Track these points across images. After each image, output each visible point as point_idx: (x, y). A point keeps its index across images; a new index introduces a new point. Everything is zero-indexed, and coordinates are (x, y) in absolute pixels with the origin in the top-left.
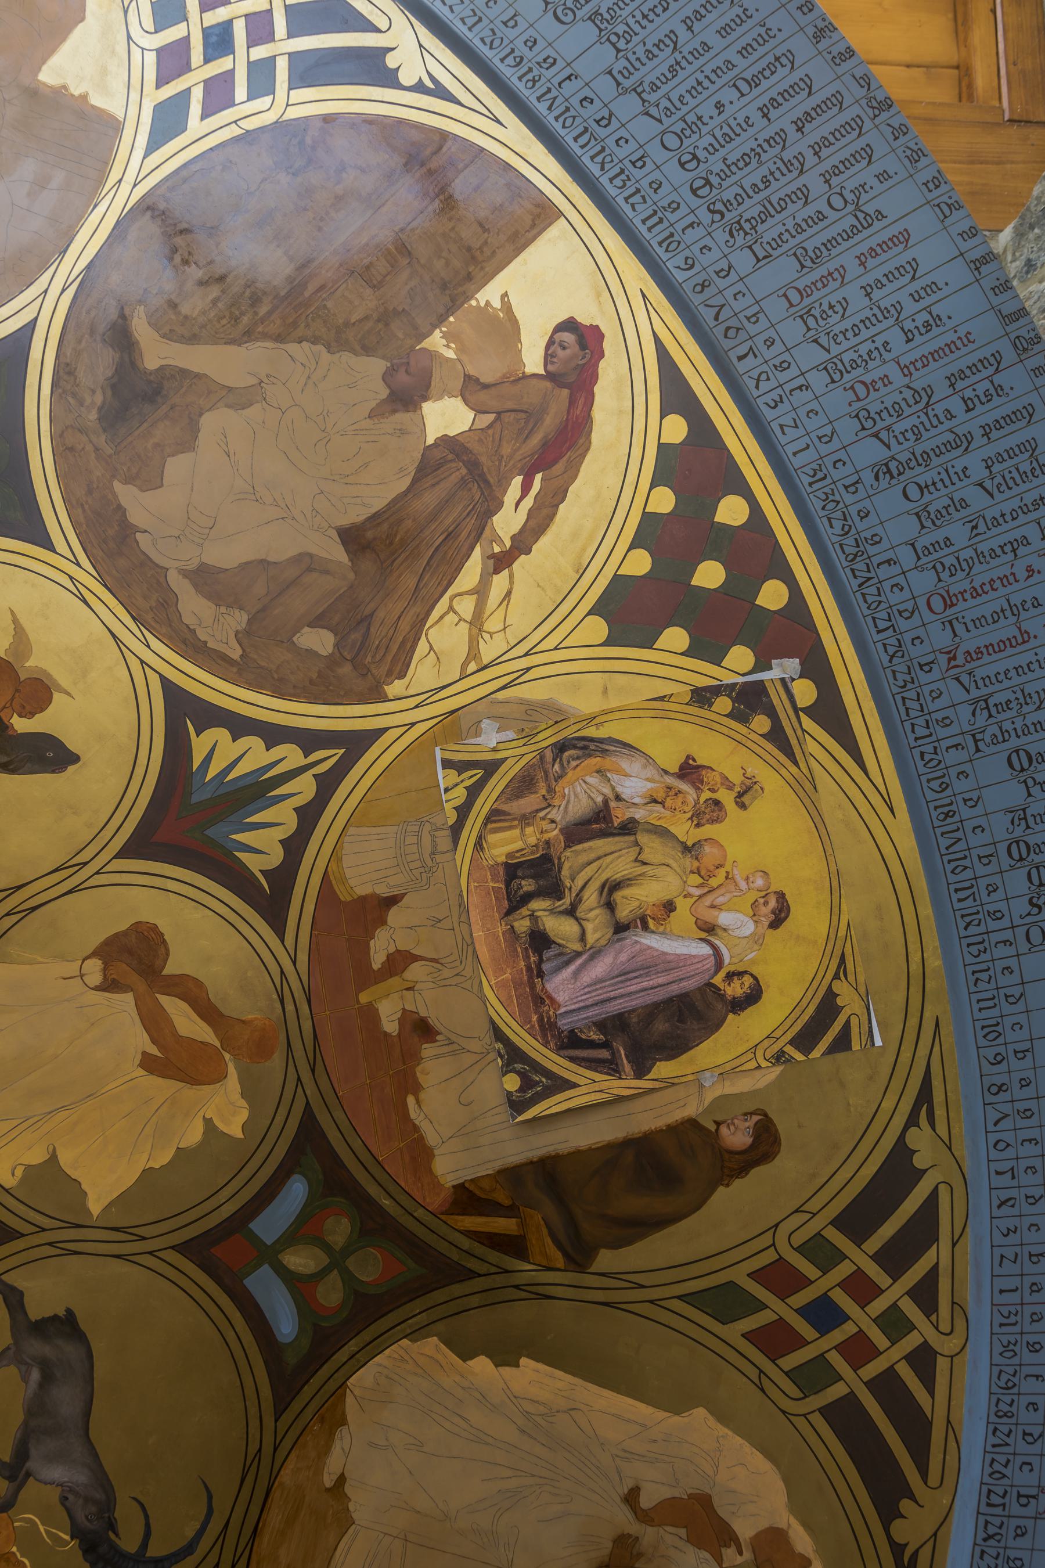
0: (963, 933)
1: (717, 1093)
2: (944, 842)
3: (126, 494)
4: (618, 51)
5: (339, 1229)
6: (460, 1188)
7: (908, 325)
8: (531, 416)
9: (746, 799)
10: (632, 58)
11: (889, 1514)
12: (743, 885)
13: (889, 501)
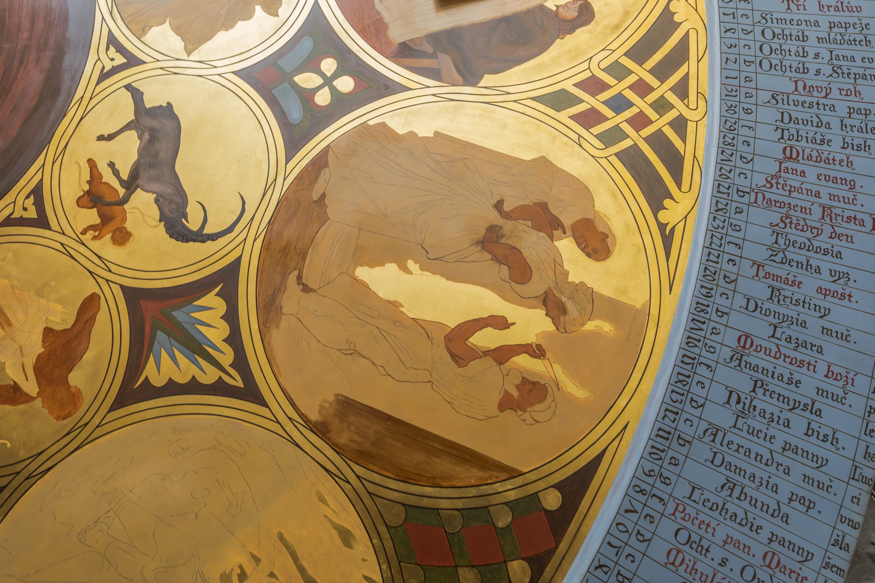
5: (329, 65)
11: (657, 206)
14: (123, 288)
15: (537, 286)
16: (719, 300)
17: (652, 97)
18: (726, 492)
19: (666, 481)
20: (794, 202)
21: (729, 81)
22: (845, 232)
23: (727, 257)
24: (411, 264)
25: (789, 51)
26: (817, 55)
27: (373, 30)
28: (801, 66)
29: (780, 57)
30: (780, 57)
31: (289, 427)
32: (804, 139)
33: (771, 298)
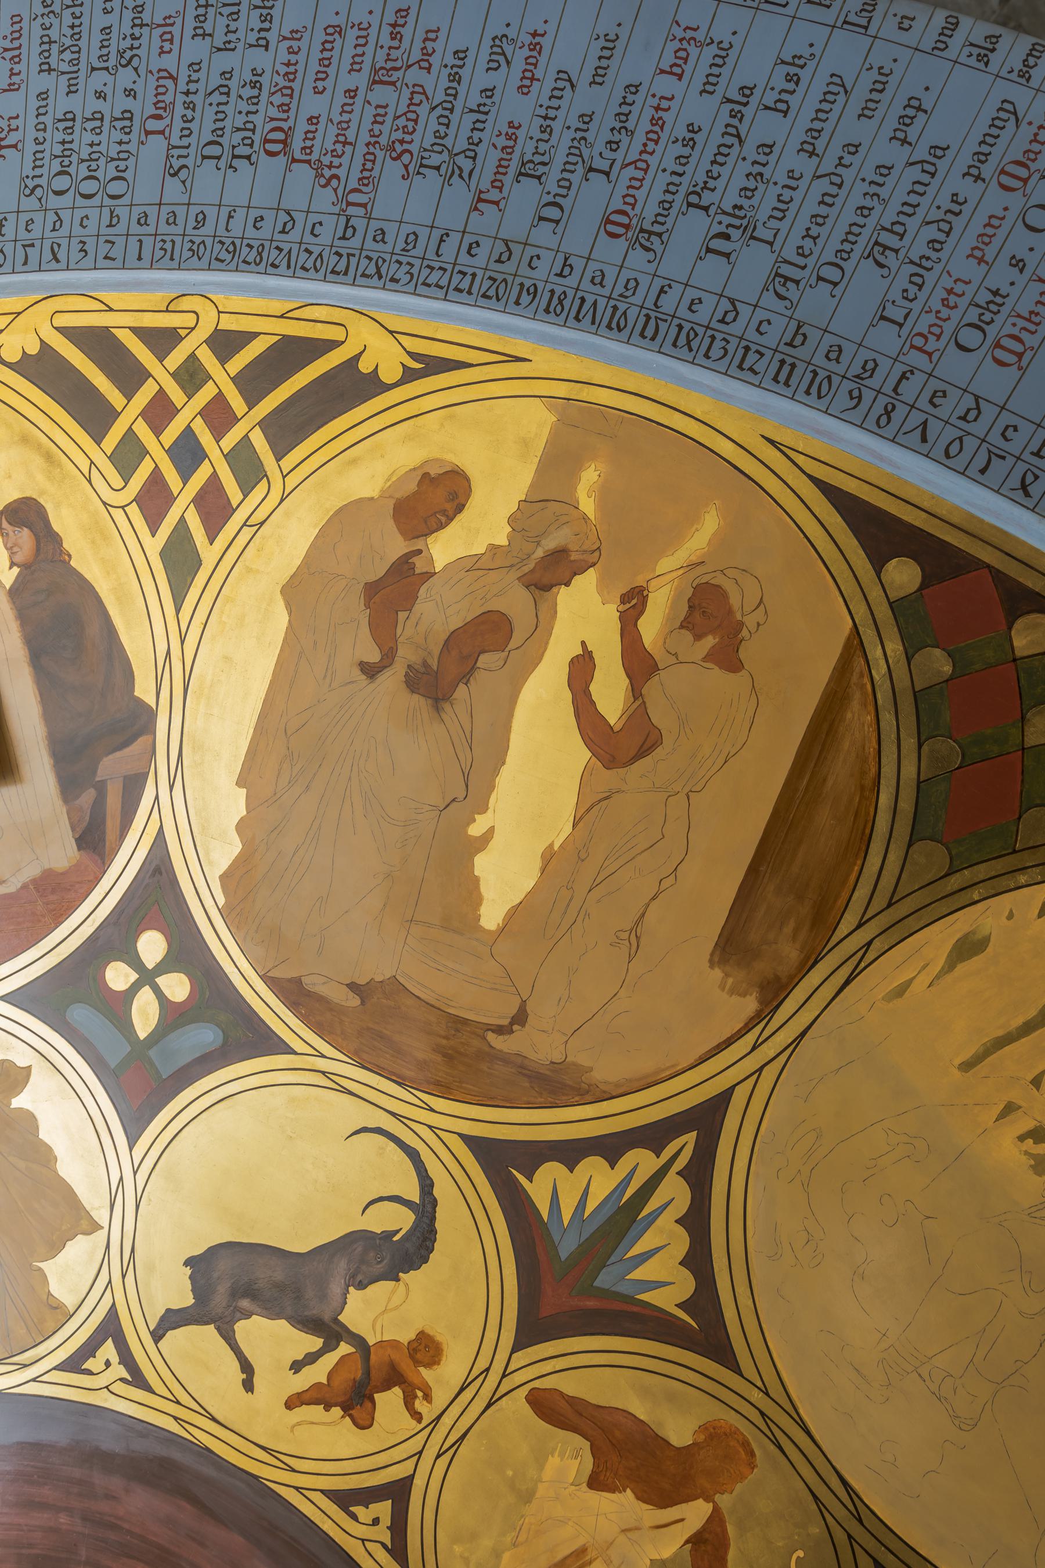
5: (118, 976)
11: (371, 385)
14: (516, 1348)
15: (515, 602)
16: (542, 270)
17: (176, 394)
18: (890, 259)
19: (870, 369)
20: (364, 137)
21: (146, 254)
22: (418, 44)
23: (464, 258)
24: (476, 830)
25: (91, 145)
26: (100, 95)
27: (56, 895)
28: (119, 124)
29: (102, 161)
30: (102, 161)
31: (769, 1050)
32: (251, 117)
33: (539, 178)
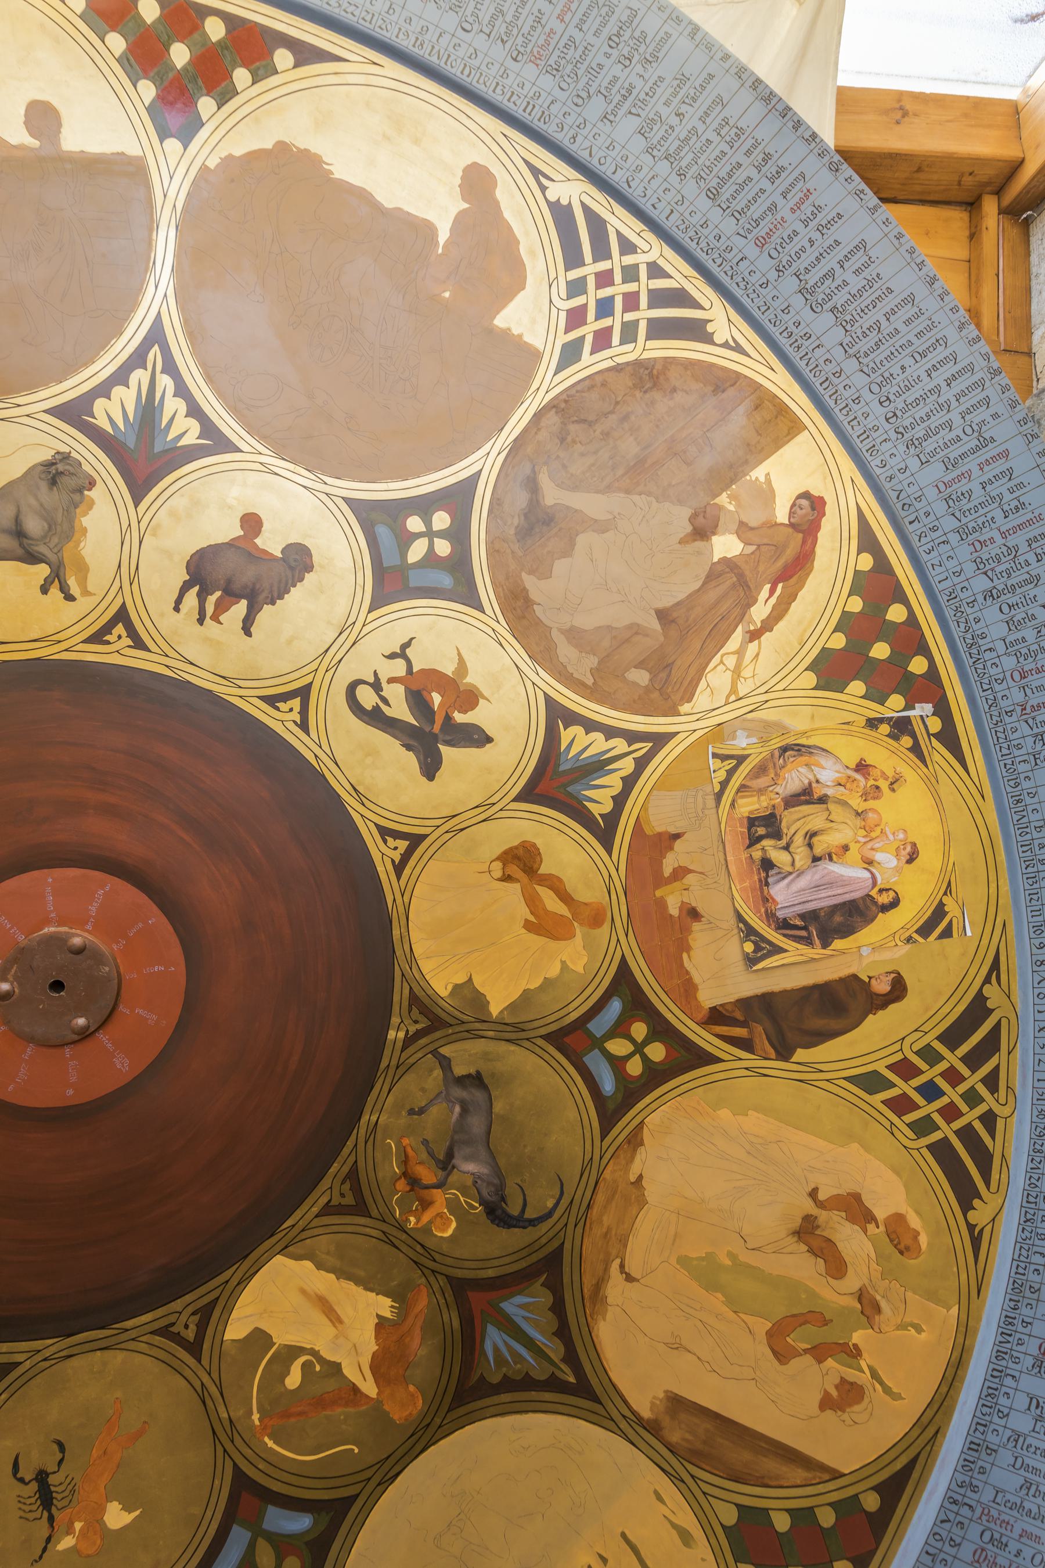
0: (1024, 871)
1: (871, 960)
2: (1016, 817)
3: (529, 581)
4: (847, 331)
5: (639, 1030)
6: (713, 1010)
7: (1006, 507)
8: (779, 549)
9: (895, 786)
10: (854, 336)
11: (966, 1206)
12: (891, 837)
13: (991, 614)
16: (1026, 1311)
18: (1024, 1491)
19: (974, 1489)
31: (623, 1424)
